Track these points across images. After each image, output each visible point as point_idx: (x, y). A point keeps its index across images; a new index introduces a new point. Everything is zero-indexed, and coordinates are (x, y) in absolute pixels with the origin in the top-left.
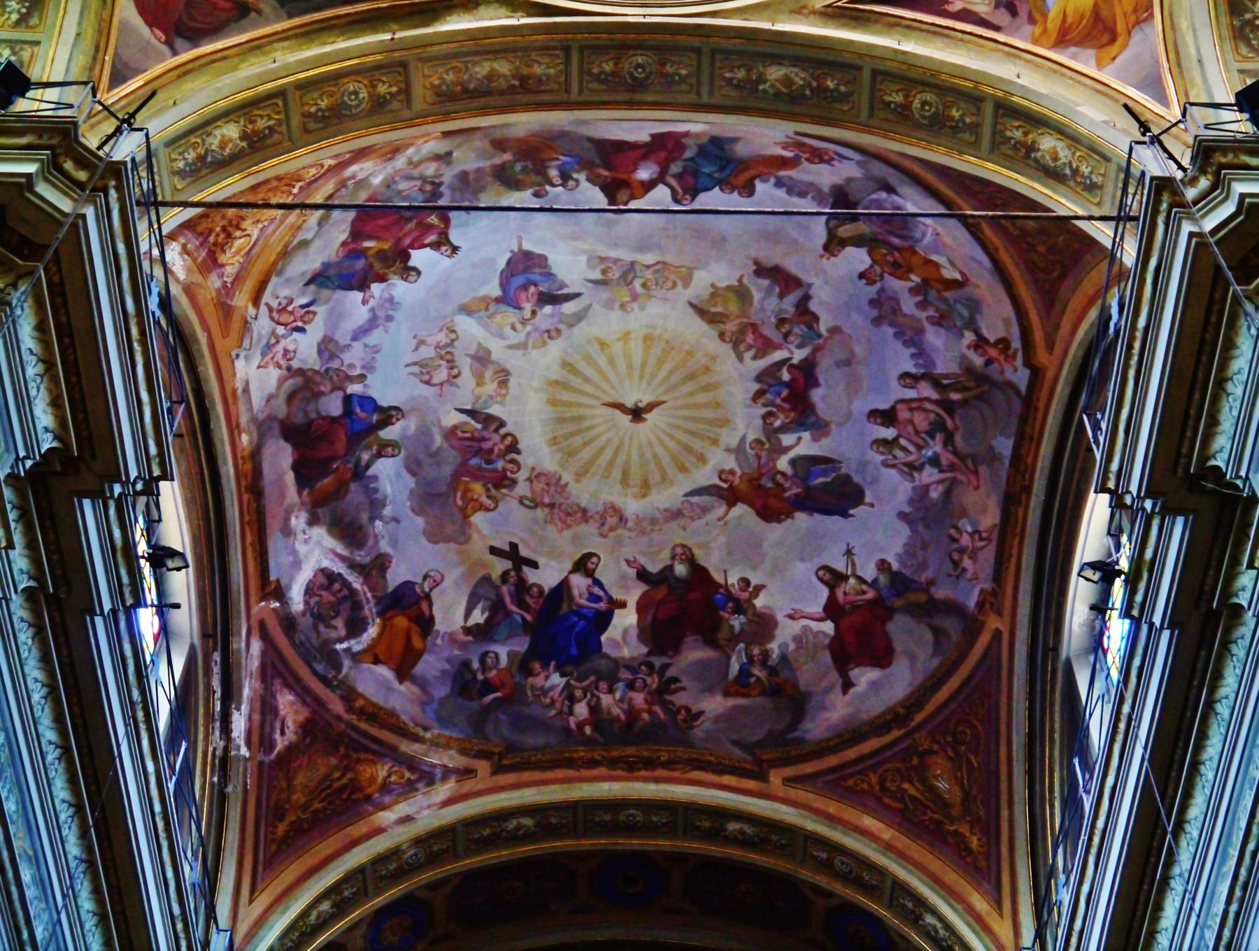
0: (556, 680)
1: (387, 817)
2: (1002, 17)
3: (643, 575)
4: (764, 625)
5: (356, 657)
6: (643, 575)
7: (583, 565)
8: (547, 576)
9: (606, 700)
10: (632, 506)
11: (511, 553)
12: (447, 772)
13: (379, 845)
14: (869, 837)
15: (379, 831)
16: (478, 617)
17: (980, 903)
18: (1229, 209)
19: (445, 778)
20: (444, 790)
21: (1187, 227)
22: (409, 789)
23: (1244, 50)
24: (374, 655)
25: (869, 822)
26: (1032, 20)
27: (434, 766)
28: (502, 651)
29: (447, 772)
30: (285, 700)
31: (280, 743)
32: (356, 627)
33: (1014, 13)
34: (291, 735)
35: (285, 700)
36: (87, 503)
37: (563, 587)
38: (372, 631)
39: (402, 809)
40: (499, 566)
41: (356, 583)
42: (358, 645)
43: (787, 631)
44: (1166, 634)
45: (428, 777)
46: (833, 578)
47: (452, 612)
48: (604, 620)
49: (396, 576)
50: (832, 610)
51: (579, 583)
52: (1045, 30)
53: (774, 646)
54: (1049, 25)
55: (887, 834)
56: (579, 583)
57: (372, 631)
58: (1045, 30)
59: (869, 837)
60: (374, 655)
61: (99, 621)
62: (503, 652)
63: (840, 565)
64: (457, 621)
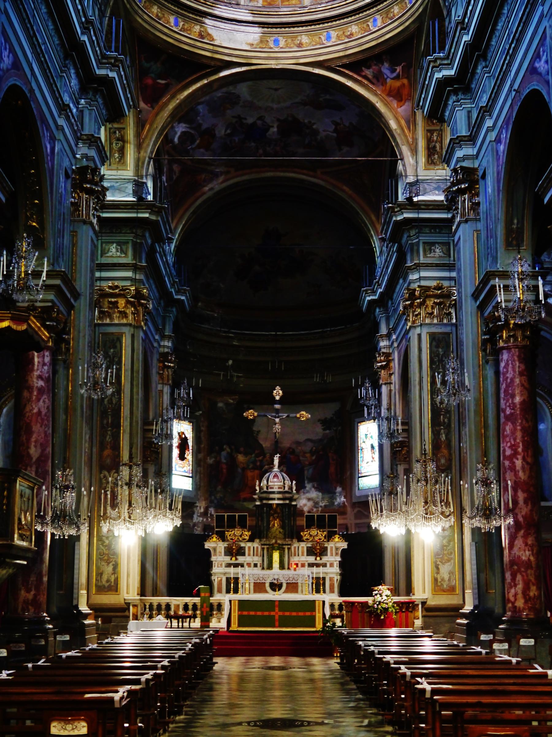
0: (253, 144)
1: (206, 189)
2: (374, 81)
3: (278, 120)
4: (316, 132)
5: (193, 149)
6: (278, 120)
7: (261, 118)
8: (250, 121)
9: (268, 149)
10: (275, 106)
11: (239, 117)
12: (222, 173)
13: (205, 197)
14: (345, 192)
15: (204, 193)
16: (229, 131)
17: (374, 218)
18: (402, 218)
19: (221, 175)
20: (221, 179)
21: (394, 219)
22: (211, 180)
23: (429, 123)
24: (199, 147)
25: (345, 188)
26: (382, 85)
27: (218, 172)
28: (237, 139)
29: (222, 173)
30: (176, 167)
31: (175, 177)
32: (193, 142)
33: (378, 81)
34: (177, 174)
35: (176, 167)
36: (156, 244)
37: (254, 124)
38: (198, 141)
39: (210, 186)
40: (234, 120)
41: (193, 132)
42: (194, 146)
43: (323, 134)
44: (395, 254)
45: (216, 176)
46: (336, 124)
47: (221, 131)
48: (267, 130)
49: (205, 126)
50: (335, 131)
51: (259, 122)
52: (385, 89)
53: (319, 137)
54: (387, 88)
55: (350, 192)
56: (259, 122)
57: (198, 141)
58: (385, 89)
59: (345, 192)
60: (199, 147)
61: (158, 254)
62: (237, 139)
63: (339, 121)
64: (223, 132)
